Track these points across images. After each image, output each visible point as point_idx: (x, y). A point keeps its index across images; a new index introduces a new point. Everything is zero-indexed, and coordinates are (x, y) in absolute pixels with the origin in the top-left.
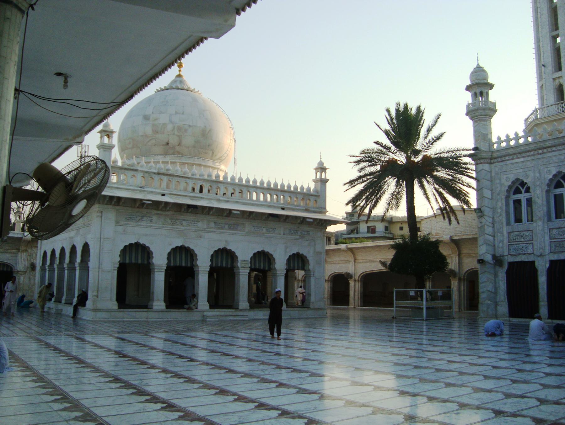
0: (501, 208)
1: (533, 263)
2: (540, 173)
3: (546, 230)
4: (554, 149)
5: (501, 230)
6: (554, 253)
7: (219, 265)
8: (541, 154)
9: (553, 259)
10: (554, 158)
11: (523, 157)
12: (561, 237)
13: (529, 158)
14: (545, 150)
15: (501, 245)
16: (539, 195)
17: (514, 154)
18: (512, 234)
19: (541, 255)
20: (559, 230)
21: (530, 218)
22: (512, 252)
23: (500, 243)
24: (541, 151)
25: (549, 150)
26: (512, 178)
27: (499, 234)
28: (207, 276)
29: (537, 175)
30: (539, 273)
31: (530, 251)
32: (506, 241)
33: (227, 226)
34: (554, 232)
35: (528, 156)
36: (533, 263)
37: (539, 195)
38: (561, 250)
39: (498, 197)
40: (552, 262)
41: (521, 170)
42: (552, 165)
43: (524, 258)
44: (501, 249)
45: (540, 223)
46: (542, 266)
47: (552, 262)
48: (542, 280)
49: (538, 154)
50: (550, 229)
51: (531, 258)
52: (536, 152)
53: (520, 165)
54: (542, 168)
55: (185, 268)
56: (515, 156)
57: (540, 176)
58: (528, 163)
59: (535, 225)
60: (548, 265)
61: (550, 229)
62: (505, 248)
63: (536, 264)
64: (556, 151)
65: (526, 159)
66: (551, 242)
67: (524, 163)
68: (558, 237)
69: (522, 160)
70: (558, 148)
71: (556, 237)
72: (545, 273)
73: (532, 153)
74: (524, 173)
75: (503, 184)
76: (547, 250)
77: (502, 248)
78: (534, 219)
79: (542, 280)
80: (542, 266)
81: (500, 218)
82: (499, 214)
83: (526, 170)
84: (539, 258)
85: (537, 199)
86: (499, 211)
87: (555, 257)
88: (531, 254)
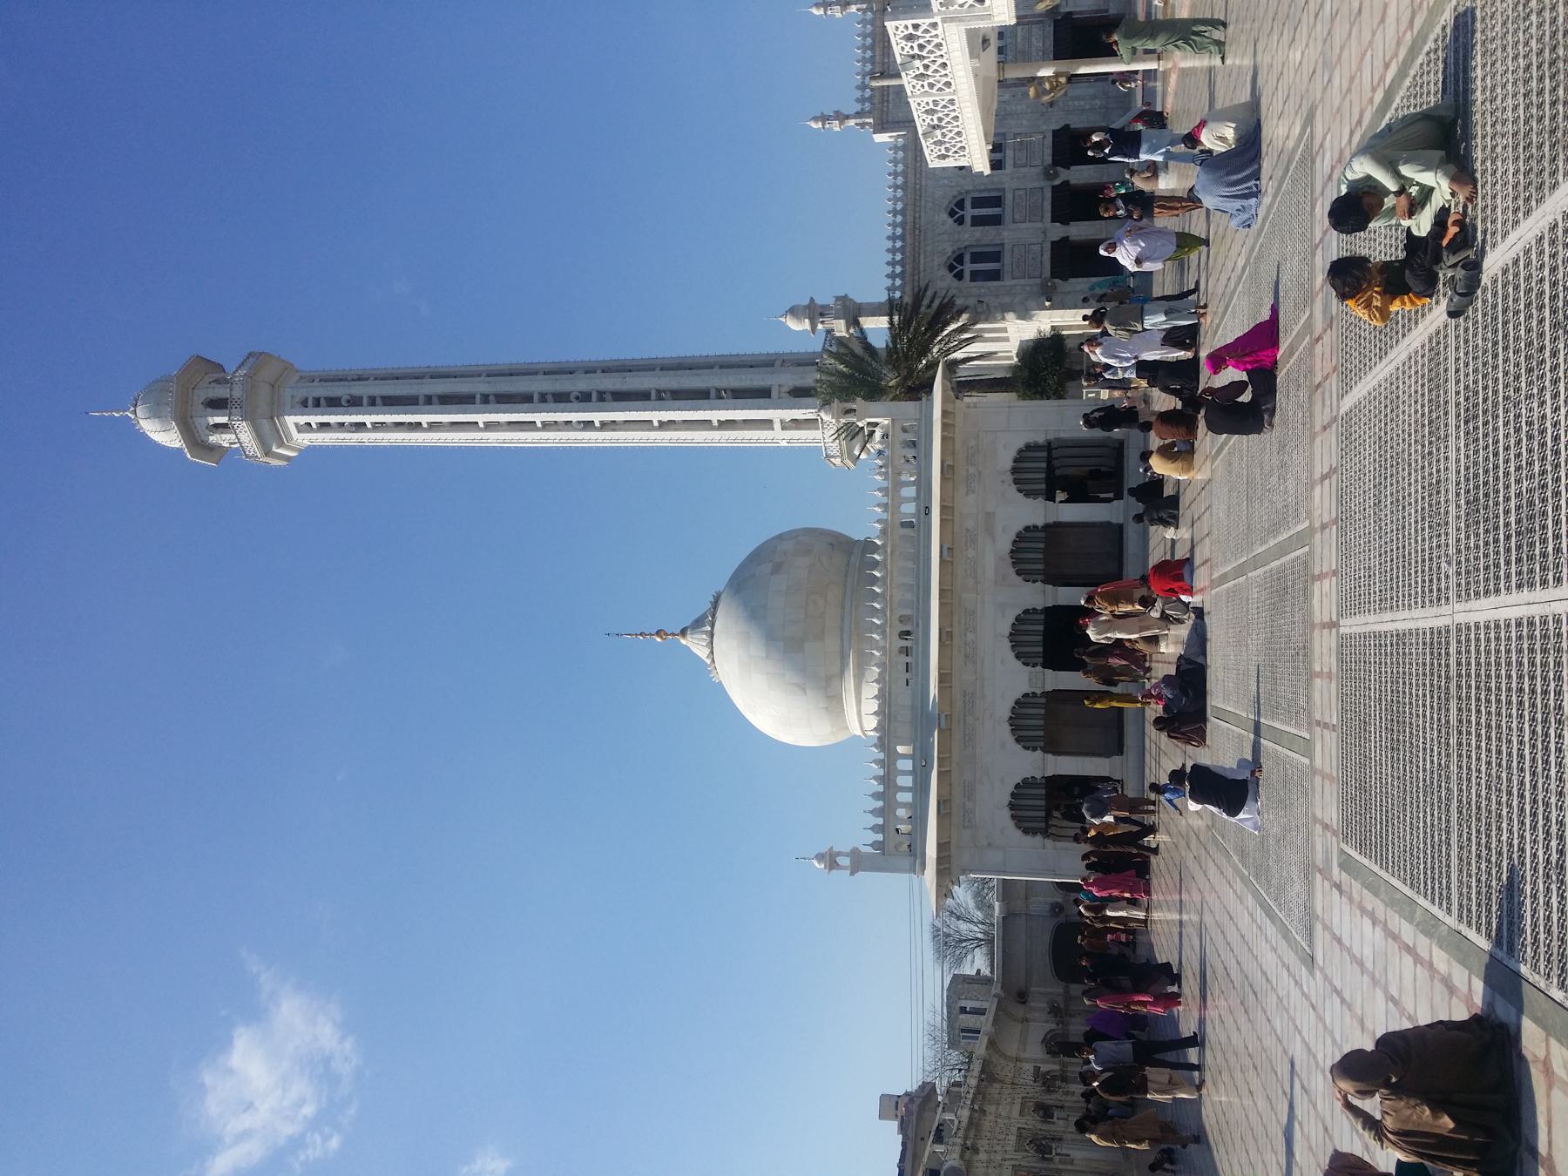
7: (1041, 733)
16: (972, 236)
22: (1037, 273)
26: (944, 272)
28: (1062, 590)
31: (1037, 248)
32: (1023, 282)
33: (971, 553)
34: (1017, 217)
37: (972, 236)
40: (1053, 221)
45: (1005, 234)
46: (1058, 231)
47: (1053, 221)
51: (1048, 246)
55: (1046, 623)
76: (1039, 225)
80: (1058, 231)
87: (1048, 215)
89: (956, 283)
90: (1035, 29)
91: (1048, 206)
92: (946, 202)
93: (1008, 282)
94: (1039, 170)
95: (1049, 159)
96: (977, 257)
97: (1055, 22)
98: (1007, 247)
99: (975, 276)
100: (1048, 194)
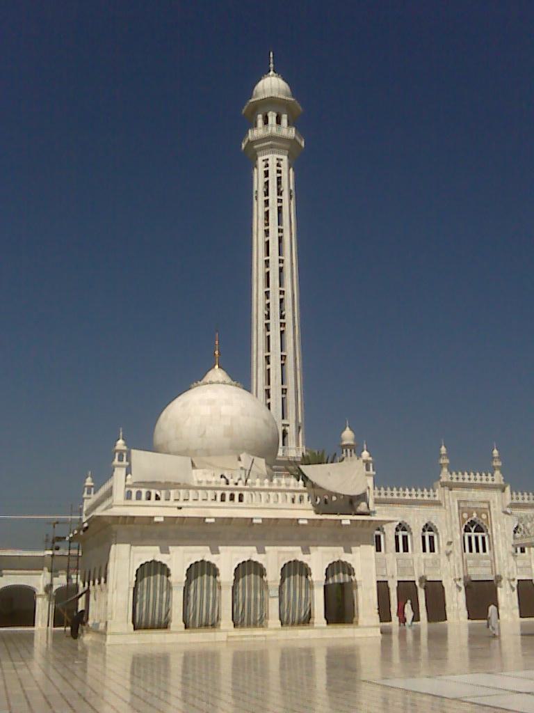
21: (406, 549)
30: (391, 590)
31: (385, 573)
51: (385, 579)
90: (489, 570)
92: (406, 521)
94: (423, 574)
100: (411, 579)
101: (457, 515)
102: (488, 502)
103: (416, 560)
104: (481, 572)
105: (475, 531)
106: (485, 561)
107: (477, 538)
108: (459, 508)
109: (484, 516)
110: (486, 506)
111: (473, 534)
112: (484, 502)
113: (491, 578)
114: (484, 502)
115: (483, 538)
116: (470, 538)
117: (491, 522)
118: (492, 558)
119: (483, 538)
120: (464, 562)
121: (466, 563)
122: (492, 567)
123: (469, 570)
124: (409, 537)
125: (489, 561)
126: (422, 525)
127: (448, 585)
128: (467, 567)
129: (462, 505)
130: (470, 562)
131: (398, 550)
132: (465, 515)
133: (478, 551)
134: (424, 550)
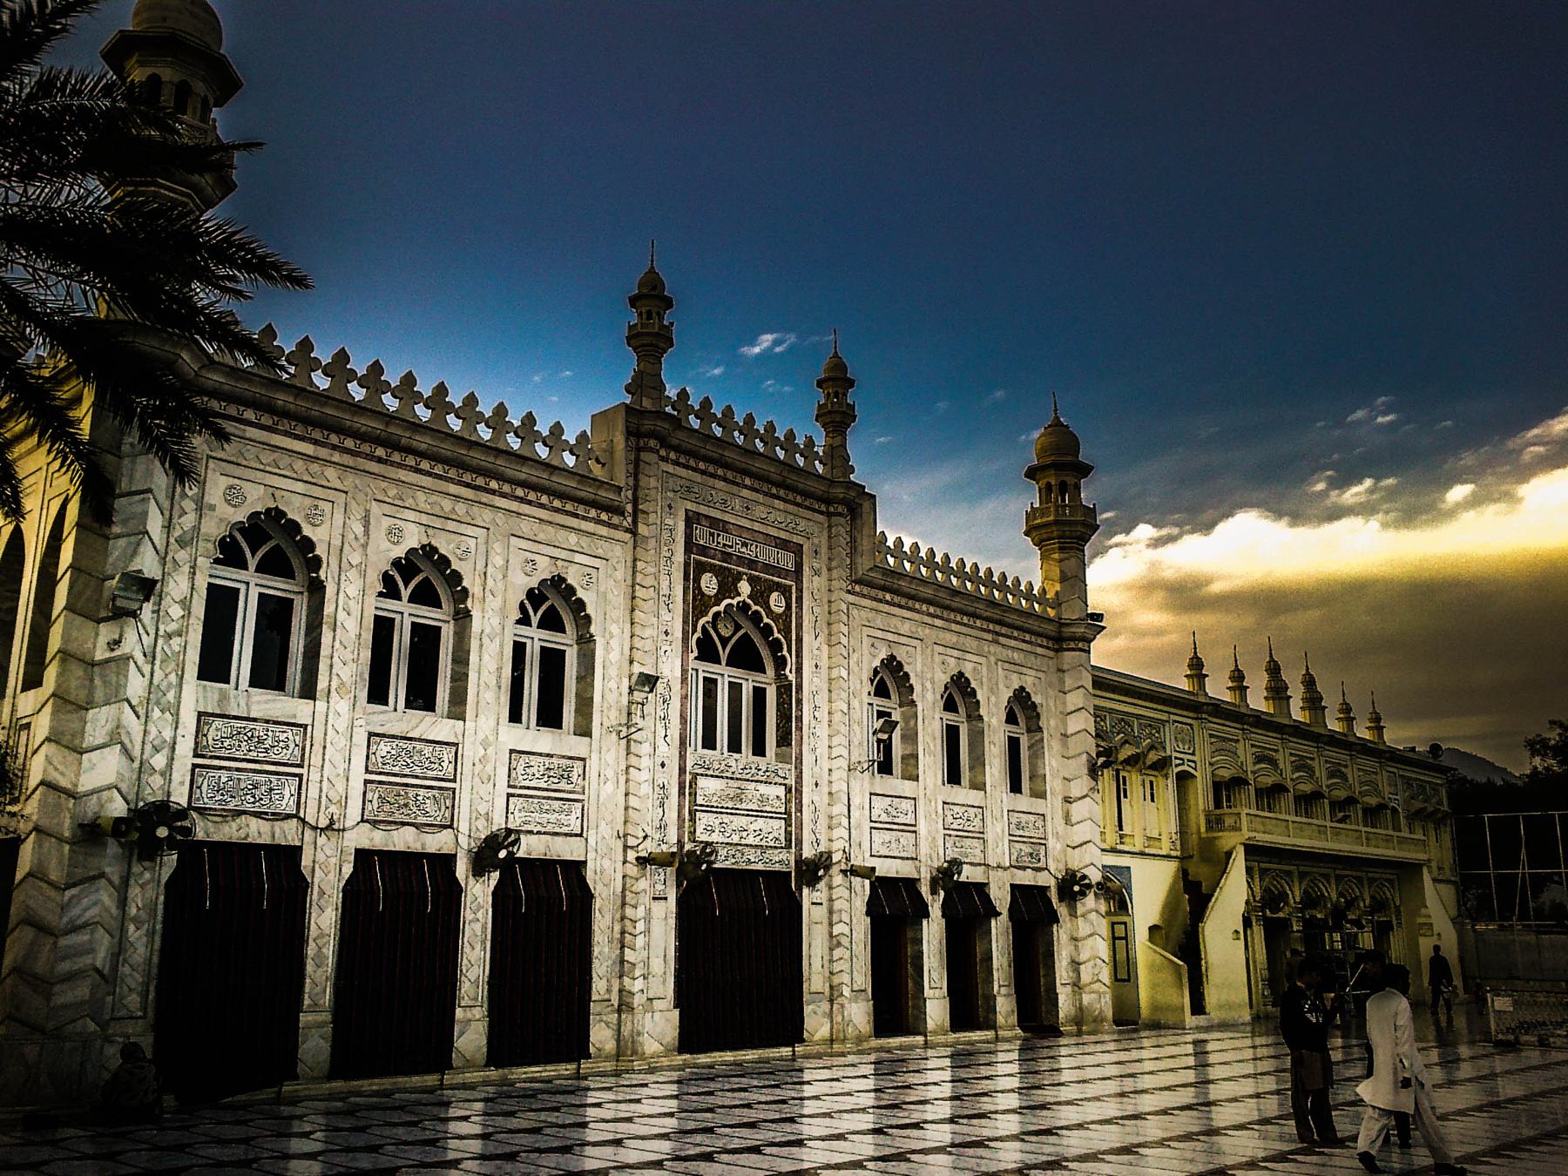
0: (186, 604)
1: (292, 854)
2: (367, 525)
3: (361, 738)
4: (425, 465)
5: (171, 696)
6: (374, 823)
8: (380, 460)
9: (365, 844)
10: (421, 496)
11: (316, 442)
12: (407, 771)
13: (336, 457)
14: (396, 457)
15: (159, 761)
16: (351, 606)
17: (285, 414)
18: (218, 723)
19: (330, 827)
20: (402, 744)
22: (206, 798)
23: (157, 750)
24: (380, 452)
25: (411, 461)
27: (157, 713)
29: (358, 528)
31: (287, 804)
32: (185, 747)
34: (384, 748)
35: (334, 447)
36: (292, 854)
37: (351, 606)
38: (398, 817)
39: (182, 555)
40: (363, 857)
41: (300, 487)
42: (411, 515)
43: (256, 831)
44: (157, 781)
45: (341, 705)
46: (327, 871)
48: (324, 920)
49: (370, 457)
50: (371, 734)
51: (287, 833)
52: (366, 448)
53: (299, 465)
54: (376, 508)
56: (285, 425)
57: (367, 533)
58: (331, 473)
59: (321, 705)
60: (348, 869)
61: (371, 734)
62: (176, 777)
63: (306, 861)
64: (429, 474)
65: (323, 452)
66: (366, 782)
67: (315, 467)
68: (396, 770)
69: (308, 448)
70: (438, 470)
71: (388, 769)
72: (336, 897)
73: (349, 443)
74: (308, 501)
75: (212, 508)
76: (354, 813)
77: (167, 772)
78: (322, 684)
79: (324, 920)
80: (327, 871)
81: (176, 642)
82: (172, 627)
83: (317, 492)
84: (322, 840)
85: (341, 615)
86: (176, 611)
87: (376, 839)
88: (289, 817)
89: (214, 528)
91: (403, 840)
93: (195, 695)
95: (530, 847)
96: (274, 615)
97: (776, 879)
98: (300, 709)
99: (221, 604)
100: (437, 843)
101: (678, 576)
102: (798, 550)
103: (470, 752)
104: (745, 837)
105: (731, 663)
106: (763, 788)
107: (735, 689)
108: (689, 546)
109: (776, 602)
110: (786, 560)
111: (725, 674)
112: (784, 545)
113: (781, 860)
114: (784, 545)
115: (759, 694)
116: (710, 685)
117: (800, 626)
118: (792, 782)
119: (759, 694)
120: (687, 787)
121: (693, 794)
122: (788, 824)
123: (703, 820)
124: (448, 633)
125: (781, 791)
126: (522, 583)
127: (606, 873)
128: (692, 814)
129: (702, 536)
130: (709, 787)
131: (378, 693)
132: (709, 584)
133: (735, 746)
134: (515, 716)
